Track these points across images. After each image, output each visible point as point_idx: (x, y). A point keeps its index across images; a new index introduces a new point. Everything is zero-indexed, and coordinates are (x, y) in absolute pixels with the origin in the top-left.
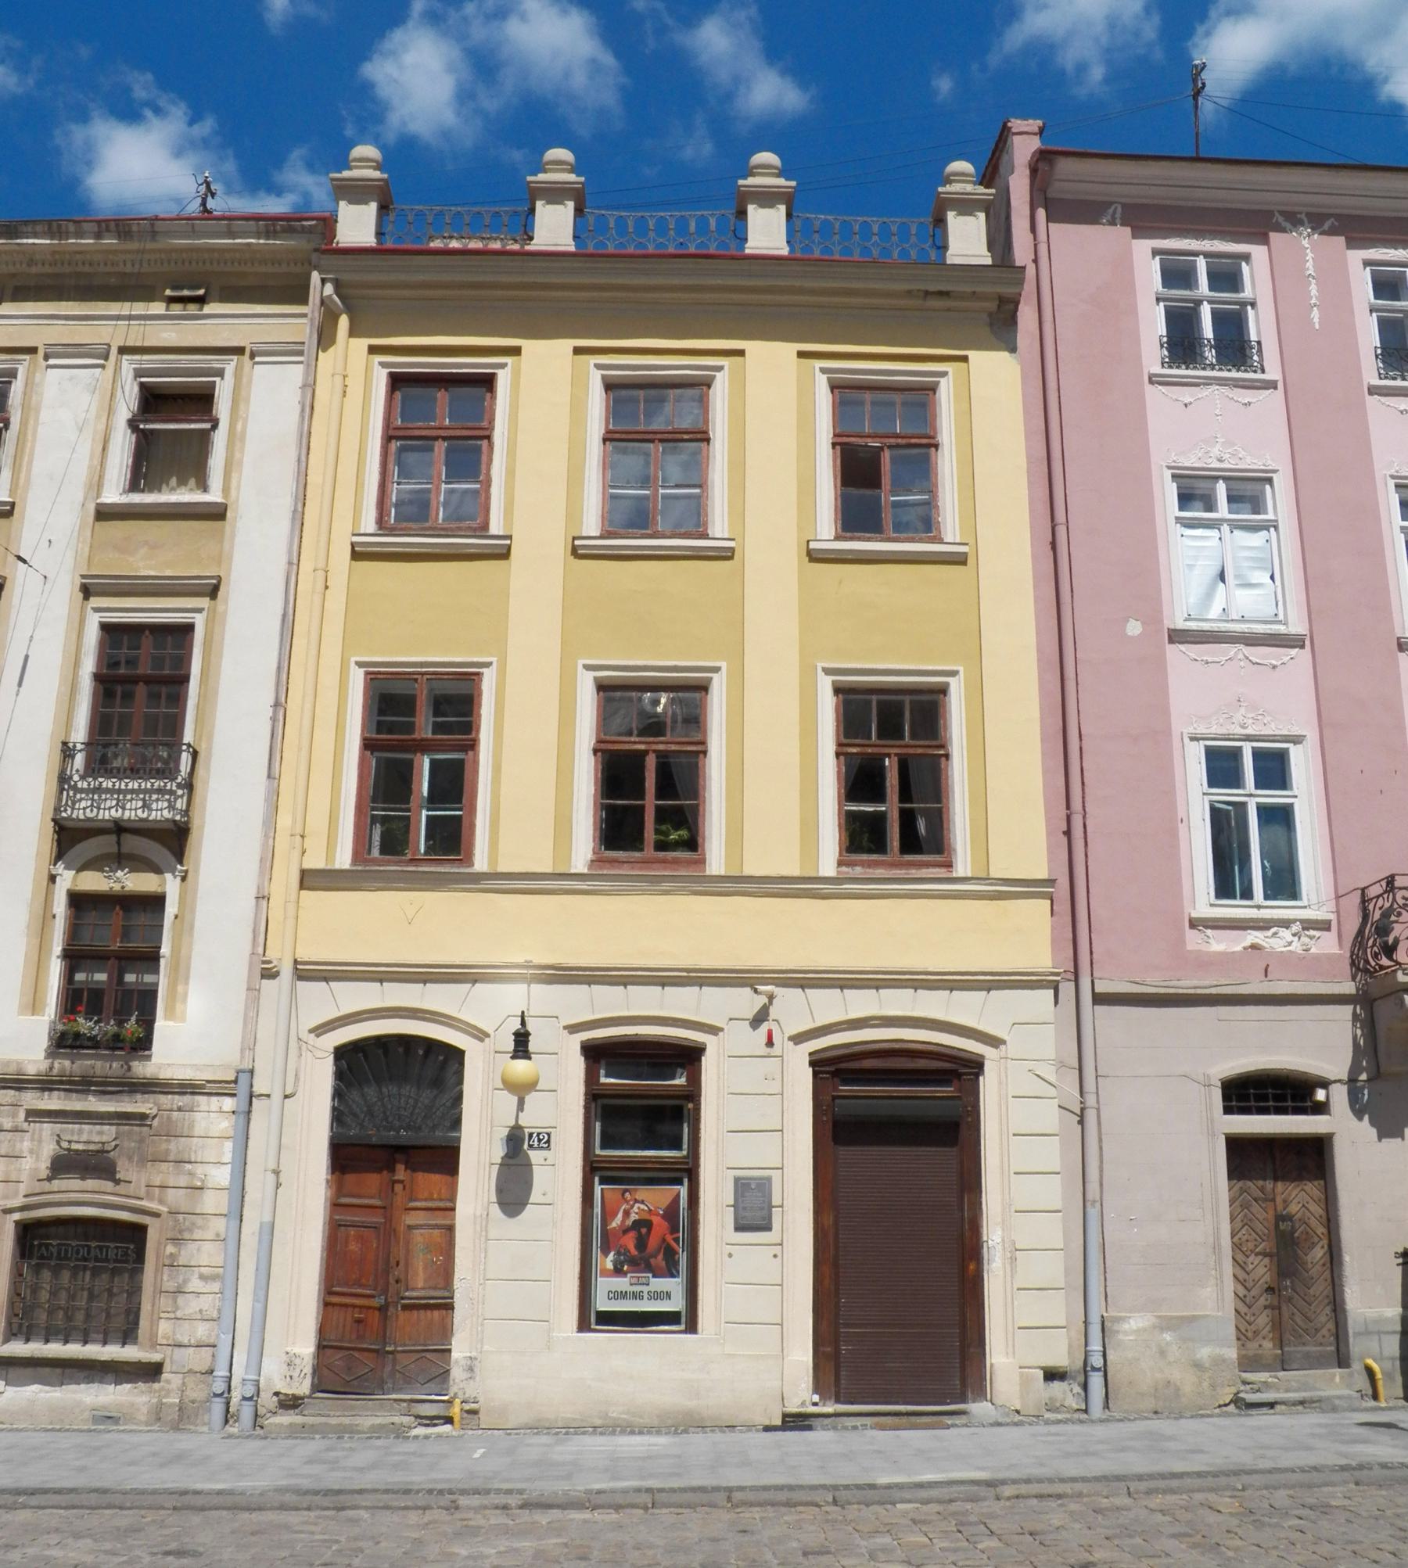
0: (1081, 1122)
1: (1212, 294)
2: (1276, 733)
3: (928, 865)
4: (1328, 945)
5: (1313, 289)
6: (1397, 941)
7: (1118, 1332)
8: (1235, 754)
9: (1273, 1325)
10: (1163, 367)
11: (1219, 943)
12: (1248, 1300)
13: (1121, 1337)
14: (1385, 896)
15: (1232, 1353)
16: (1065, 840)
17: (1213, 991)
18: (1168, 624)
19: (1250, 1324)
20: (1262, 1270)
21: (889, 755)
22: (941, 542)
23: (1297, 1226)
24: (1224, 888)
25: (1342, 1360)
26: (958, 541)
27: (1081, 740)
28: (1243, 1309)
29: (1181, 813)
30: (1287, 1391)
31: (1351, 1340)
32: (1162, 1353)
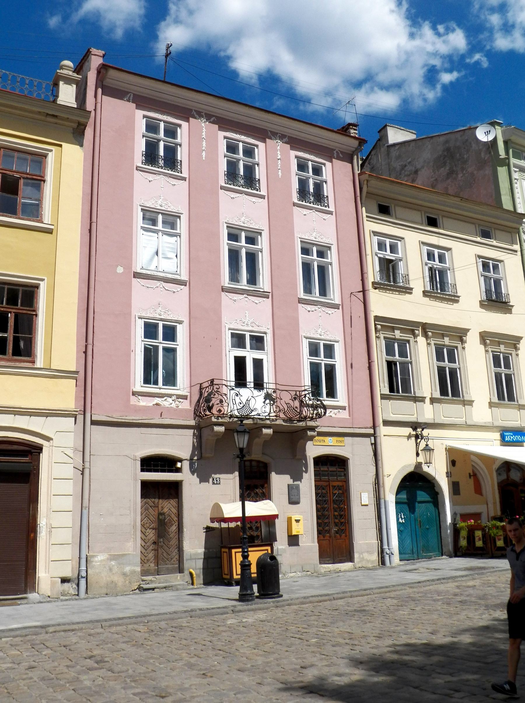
0: (82, 474)
1: (165, 138)
2: (173, 319)
3: (24, 361)
4: (186, 405)
5: (204, 144)
6: (213, 405)
7: (93, 561)
8: (156, 326)
9: (155, 558)
10: (142, 164)
11: (144, 402)
12: (145, 547)
13: (94, 563)
14: (210, 387)
15: (138, 569)
16: (84, 355)
17: (140, 421)
18: (134, 270)
19: (146, 557)
20: (152, 535)
21: (11, 312)
22: (42, 222)
23: (166, 517)
24: (147, 381)
25: (181, 570)
26: (50, 223)
27: (94, 314)
28: (144, 551)
29: (132, 348)
30: (159, 583)
31: (185, 562)
32: (111, 570)
